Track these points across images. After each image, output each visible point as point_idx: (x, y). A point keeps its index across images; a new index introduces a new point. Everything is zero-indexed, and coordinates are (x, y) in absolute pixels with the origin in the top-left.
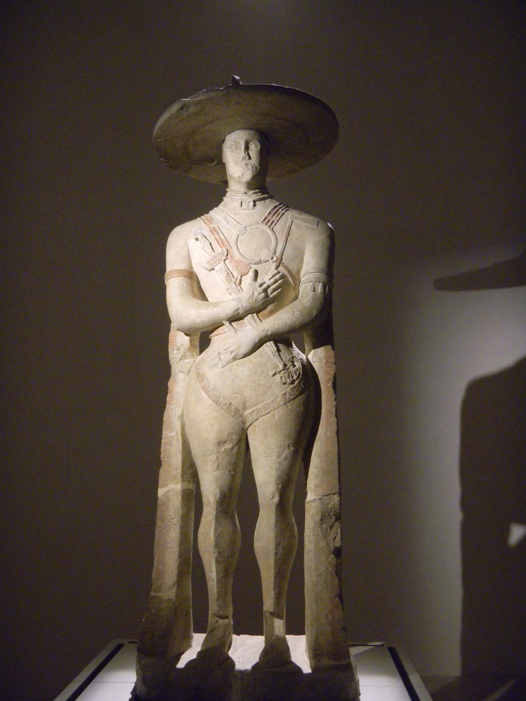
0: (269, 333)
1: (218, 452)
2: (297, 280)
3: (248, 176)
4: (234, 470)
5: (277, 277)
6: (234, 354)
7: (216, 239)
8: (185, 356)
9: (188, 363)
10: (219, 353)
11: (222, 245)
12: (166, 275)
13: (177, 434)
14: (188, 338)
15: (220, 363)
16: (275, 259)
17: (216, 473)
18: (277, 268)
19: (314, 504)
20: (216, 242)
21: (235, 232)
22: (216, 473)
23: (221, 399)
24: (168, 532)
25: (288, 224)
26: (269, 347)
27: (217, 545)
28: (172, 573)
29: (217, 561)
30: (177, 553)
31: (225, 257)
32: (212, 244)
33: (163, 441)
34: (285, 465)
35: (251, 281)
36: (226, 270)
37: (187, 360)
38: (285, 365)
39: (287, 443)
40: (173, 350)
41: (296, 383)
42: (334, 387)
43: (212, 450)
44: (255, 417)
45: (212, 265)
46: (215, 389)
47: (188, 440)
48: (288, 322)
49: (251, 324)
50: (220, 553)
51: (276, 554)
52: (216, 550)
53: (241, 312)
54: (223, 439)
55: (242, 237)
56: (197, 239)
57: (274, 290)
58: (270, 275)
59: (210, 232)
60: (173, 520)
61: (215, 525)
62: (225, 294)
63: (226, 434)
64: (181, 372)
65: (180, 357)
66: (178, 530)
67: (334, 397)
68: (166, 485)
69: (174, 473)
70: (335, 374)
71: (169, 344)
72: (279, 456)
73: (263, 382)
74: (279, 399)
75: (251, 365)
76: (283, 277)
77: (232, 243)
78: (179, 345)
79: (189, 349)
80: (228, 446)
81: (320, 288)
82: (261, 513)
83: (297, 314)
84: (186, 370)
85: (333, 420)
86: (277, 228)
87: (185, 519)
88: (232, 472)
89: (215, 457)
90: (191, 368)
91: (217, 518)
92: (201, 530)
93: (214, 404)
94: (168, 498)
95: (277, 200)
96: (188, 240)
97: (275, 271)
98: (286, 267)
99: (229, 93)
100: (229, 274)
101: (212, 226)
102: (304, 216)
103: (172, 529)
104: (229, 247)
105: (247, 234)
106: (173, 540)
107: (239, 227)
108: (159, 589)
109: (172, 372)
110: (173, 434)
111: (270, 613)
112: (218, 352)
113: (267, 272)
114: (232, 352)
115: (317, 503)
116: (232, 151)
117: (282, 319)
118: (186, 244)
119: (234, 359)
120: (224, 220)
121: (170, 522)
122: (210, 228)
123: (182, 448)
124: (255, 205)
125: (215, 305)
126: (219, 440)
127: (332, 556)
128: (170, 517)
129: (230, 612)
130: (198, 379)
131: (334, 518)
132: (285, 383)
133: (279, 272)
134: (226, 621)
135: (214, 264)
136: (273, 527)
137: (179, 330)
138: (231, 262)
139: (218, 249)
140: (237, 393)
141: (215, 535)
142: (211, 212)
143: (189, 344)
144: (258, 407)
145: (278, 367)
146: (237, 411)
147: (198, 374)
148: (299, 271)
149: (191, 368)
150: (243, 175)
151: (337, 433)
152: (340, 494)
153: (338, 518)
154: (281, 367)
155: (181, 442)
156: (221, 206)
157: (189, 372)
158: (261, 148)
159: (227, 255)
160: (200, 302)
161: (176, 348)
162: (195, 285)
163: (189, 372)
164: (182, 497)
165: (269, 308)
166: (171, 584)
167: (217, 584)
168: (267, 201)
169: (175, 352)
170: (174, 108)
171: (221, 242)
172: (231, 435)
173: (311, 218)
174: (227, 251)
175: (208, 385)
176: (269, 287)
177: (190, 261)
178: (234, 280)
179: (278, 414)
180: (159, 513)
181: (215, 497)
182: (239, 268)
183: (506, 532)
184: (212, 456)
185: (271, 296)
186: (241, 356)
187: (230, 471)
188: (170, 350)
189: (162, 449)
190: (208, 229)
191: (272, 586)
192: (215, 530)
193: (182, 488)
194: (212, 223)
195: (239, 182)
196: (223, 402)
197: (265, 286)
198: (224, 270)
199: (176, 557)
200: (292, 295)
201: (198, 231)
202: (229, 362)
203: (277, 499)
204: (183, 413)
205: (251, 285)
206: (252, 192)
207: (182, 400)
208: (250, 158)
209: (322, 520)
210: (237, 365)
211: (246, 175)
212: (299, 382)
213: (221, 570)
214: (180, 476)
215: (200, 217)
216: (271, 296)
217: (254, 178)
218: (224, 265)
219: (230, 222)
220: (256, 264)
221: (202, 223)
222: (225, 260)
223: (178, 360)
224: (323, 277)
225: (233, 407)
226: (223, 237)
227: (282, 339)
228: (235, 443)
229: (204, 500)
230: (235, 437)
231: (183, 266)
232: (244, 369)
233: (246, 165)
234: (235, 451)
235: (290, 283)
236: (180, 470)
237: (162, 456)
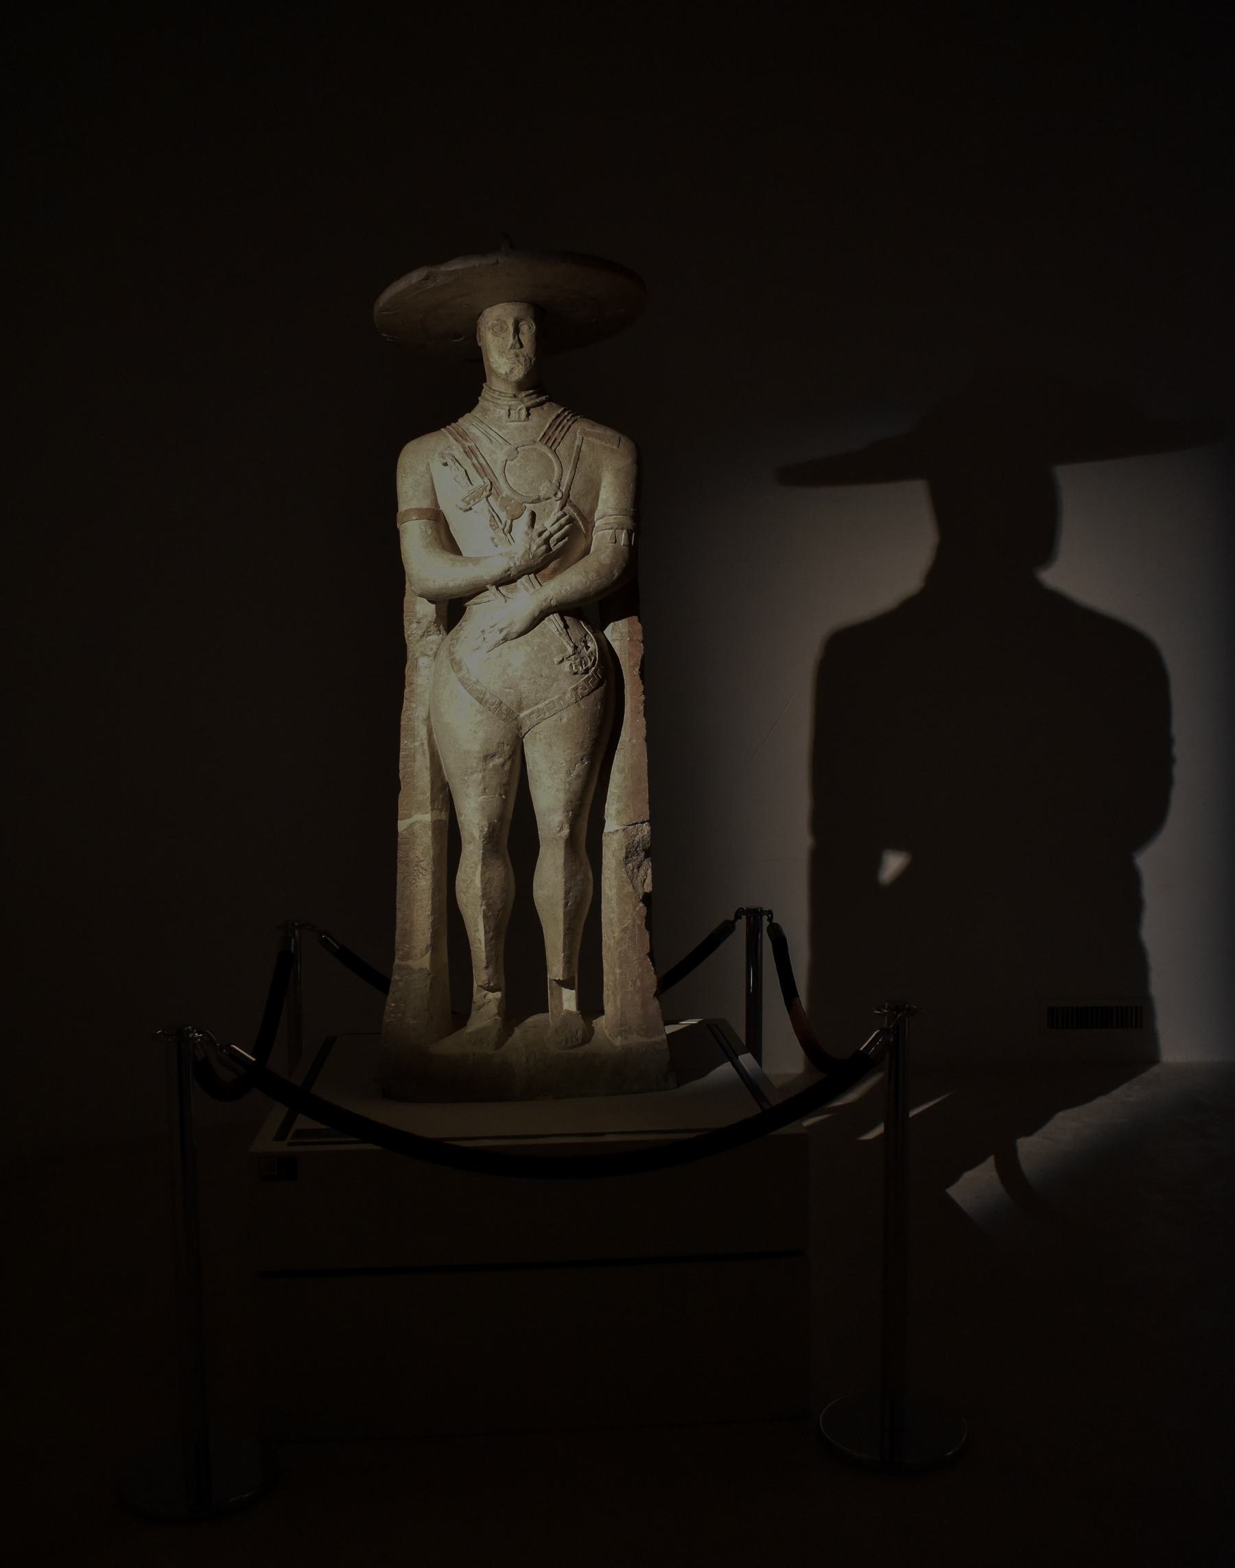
0: (553, 603)
2: (589, 522)
3: (519, 373)
4: (506, 793)
5: (563, 520)
6: (504, 633)
9: (433, 642)
12: (399, 516)
13: (422, 744)
16: (560, 495)
18: (562, 509)
19: (615, 837)
21: (501, 456)
25: (577, 443)
26: (553, 623)
27: (484, 896)
29: (485, 916)
30: (429, 907)
33: (402, 754)
34: (577, 785)
35: (526, 528)
38: (576, 647)
39: (579, 754)
40: (411, 623)
41: (591, 672)
42: (642, 675)
44: (535, 718)
48: (580, 587)
49: (527, 590)
50: (488, 906)
51: (566, 905)
53: (513, 573)
54: (491, 752)
56: (446, 464)
57: (559, 540)
58: (553, 518)
62: (489, 547)
65: (420, 633)
66: (429, 877)
67: (642, 688)
68: (410, 816)
69: (420, 798)
70: (643, 657)
72: (569, 773)
73: (546, 672)
74: (569, 695)
75: (529, 649)
76: (571, 520)
77: (498, 471)
78: (419, 616)
80: (498, 761)
81: (623, 536)
82: (542, 850)
83: (592, 575)
84: (431, 653)
85: (642, 721)
86: (561, 450)
87: (436, 860)
89: (480, 776)
92: (460, 875)
95: (560, 404)
97: (560, 513)
98: (574, 507)
99: (497, 262)
100: (494, 517)
101: (467, 444)
102: (599, 430)
107: (507, 447)
108: (408, 956)
109: (410, 655)
111: (558, 982)
113: (548, 515)
114: (501, 631)
115: (621, 834)
116: (495, 334)
117: (570, 582)
119: (505, 640)
122: (463, 447)
124: (528, 415)
125: (476, 561)
127: (641, 904)
129: (503, 985)
131: (643, 854)
132: (576, 673)
133: (565, 514)
134: (498, 995)
136: (561, 869)
139: (478, 481)
142: (461, 421)
144: (539, 706)
145: (566, 650)
146: (510, 712)
147: (452, 660)
148: (592, 512)
150: (512, 371)
151: (648, 739)
152: (650, 822)
153: (648, 853)
154: (570, 650)
155: (428, 755)
156: (477, 412)
157: (436, 654)
158: (537, 330)
160: (452, 556)
162: (442, 531)
163: (436, 654)
164: (433, 833)
165: (552, 565)
168: (545, 407)
169: (415, 625)
170: (415, 277)
171: (482, 470)
173: (610, 433)
176: (551, 535)
177: (435, 494)
178: (501, 526)
179: (566, 717)
180: (400, 854)
183: (877, 863)
185: (554, 549)
188: (406, 624)
189: (401, 766)
191: (560, 945)
192: (483, 874)
195: (506, 380)
197: (546, 534)
200: (582, 545)
202: (497, 645)
203: (566, 831)
205: (527, 534)
206: (523, 394)
207: (427, 696)
208: (522, 346)
209: (627, 857)
211: (516, 372)
212: (595, 671)
216: (554, 549)
217: (528, 375)
224: (628, 522)
225: (504, 708)
227: (570, 610)
229: (464, 835)
230: (506, 748)
231: (426, 504)
232: (519, 654)
233: (517, 356)
234: (507, 768)
235: (579, 528)
236: (429, 794)
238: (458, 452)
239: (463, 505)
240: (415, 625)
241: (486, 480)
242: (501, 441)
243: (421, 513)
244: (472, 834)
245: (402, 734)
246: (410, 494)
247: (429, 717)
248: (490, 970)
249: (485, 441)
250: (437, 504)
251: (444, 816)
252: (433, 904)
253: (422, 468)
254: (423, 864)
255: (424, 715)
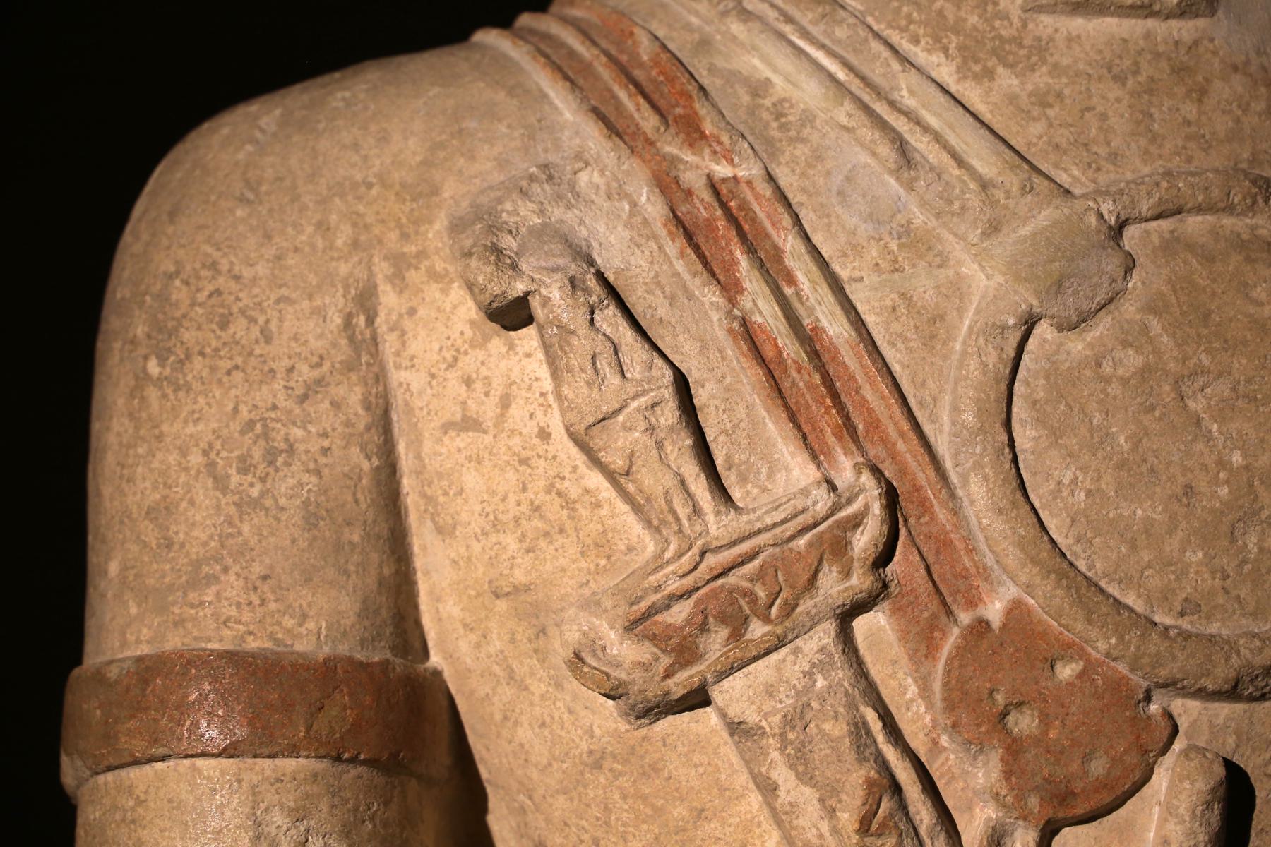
7: (749, 336)
11: (827, 421)
12: (84, 705)
20: (748, 377)
21: (984, 282)
31: (860, 581)
32: (701, 397)
36: (859, 730)
45: (685, 653)
55: (1077, 345)
56: (512, 315)
59: (674, 247)
77: (952, 417)
96: (389, 299)
101: (698, 168)
104: (907, 448)
105: (1129, 309)
118: (363, 347)
120: (844, 113)
122: (667, 184)
135: (716, 644)
138: (923, 640)
139: (784, 477)
159: (884, 557)
171: (818, 389)
174: (891, 498)
177: (397, 544)
182: (1024, 723)
190: (653, 208)
194: (693, 133)
198: (838, 729)
201: (525, 213)
215: (504, 21)
218: (842, 674)
219: (920, 143)
220: (1232, 693)
221: (565, 108)
222: (847, 615)
226: (835, 328)
231: (316, 621)
238: (621, 224)
239: (626, 653)
241: (846, 469)
242: (985, 159)
243: (275, 699)
246: (192, 524)
249: (863, 156)
250: (405, 628)
253: (308, 328)
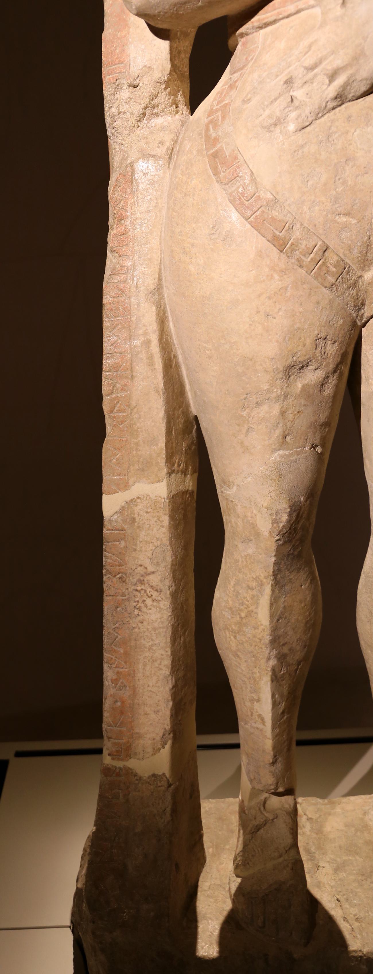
1: (286, 397)
6: (340, 80)
8: (154, 107)
9: (163, 129)
10: (289, 82)
14: (164, 45)
15: (293, 115)
17: (276, 456)
22: (276, 456)
23: (297, 233)
24: (139, 609)
27: (275, 641)
28: (157, 712)
29: (275, 678)
30: (167, 662)
33: (107, 363)
37: (159, 121)
40: (117, 88)
43: (269, 391)
46: (276, 201)
47: (175, 356)
50: (282, 658)
52: (274, 652)
54: (300, 358)
60: (151, 577)
61: (273, 591)
63: (308, 342)
64: (145, 156)
65: (137, 109)
66: (166, 604)
68: (126, 487)
71: (104, 71)
78: (135, 70)
79: (168, 84)
80: (312, 376)
84: (162, 151)
87: (178, 570)
88: (319, 449)
89: (276, 410)
90: (175, 142)
91: (275, 574)
92: (223, 598)
93: (274, 252)
94: (134, 520)
103: (149, 602)
106: (155, 629)
110: (137, 342)
112: (283, 77)
119: (341, 99)
121: (141, 582)
123: (165, 384)
126: (290, 361)
128: (140, 570)
130: (216, 173)
137: (139, 15)
140: (347, 214)
141: (271, 616)
143: (168, 66)
149: (175, 142)
161: (125, 82)
164: (172, 518)
166: (158, 738)
167: (273, 728)
169: (125, 93)
172: (321, 343)
175: (251, 189)
180: (109, 559)
181: (275, 522)
184: (265, 407)
186: (363, 89)
187: (314, 447)
192: (274, 602)
193: (169, 493)
196: (303, 245)
199: (166, 671)
204: (160, 279)
210: (349, 118)
213: (281, 696)
214: (162, 461)
223: (133, 120)
228: (332, 366)
234: (329, 390)
237: (106, 407)
240: (125, 93)
244: (253, 526)
245: (106, 323)
247: (159, 288)
248: (279, 765)
251: (189, 483)
252: (173, 654)
254: (154, 580)
255: (151, 282)
